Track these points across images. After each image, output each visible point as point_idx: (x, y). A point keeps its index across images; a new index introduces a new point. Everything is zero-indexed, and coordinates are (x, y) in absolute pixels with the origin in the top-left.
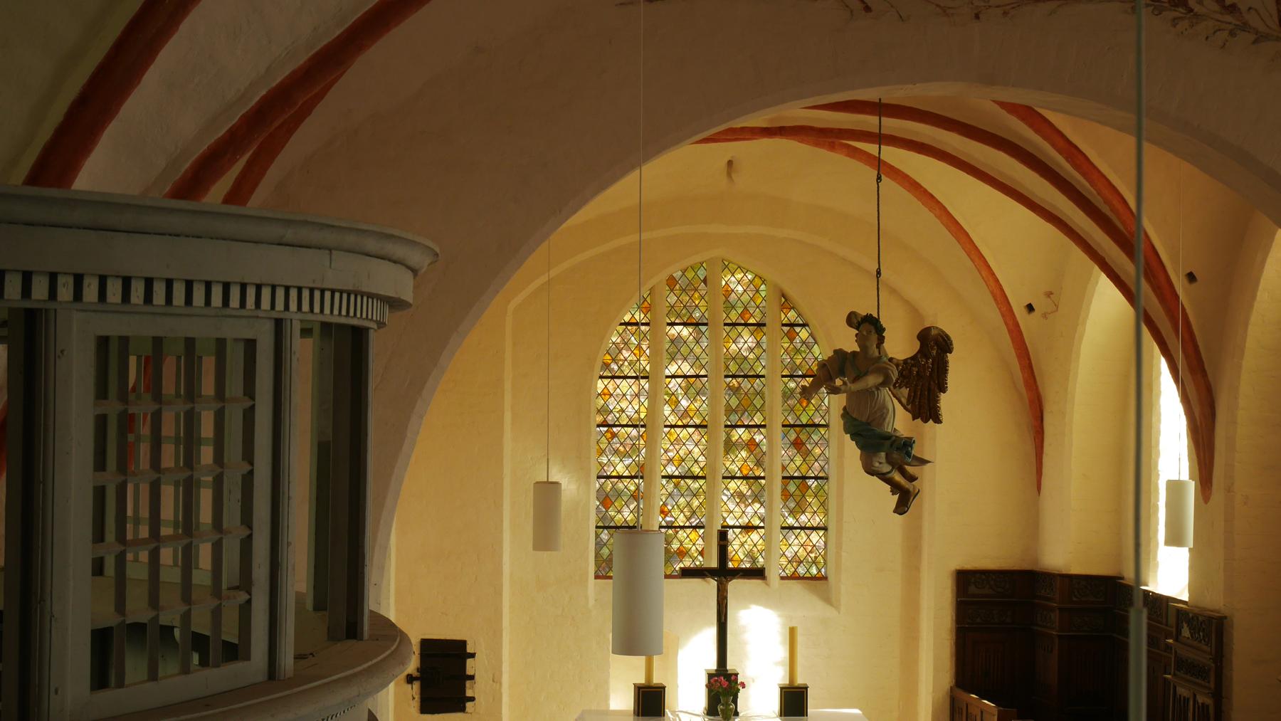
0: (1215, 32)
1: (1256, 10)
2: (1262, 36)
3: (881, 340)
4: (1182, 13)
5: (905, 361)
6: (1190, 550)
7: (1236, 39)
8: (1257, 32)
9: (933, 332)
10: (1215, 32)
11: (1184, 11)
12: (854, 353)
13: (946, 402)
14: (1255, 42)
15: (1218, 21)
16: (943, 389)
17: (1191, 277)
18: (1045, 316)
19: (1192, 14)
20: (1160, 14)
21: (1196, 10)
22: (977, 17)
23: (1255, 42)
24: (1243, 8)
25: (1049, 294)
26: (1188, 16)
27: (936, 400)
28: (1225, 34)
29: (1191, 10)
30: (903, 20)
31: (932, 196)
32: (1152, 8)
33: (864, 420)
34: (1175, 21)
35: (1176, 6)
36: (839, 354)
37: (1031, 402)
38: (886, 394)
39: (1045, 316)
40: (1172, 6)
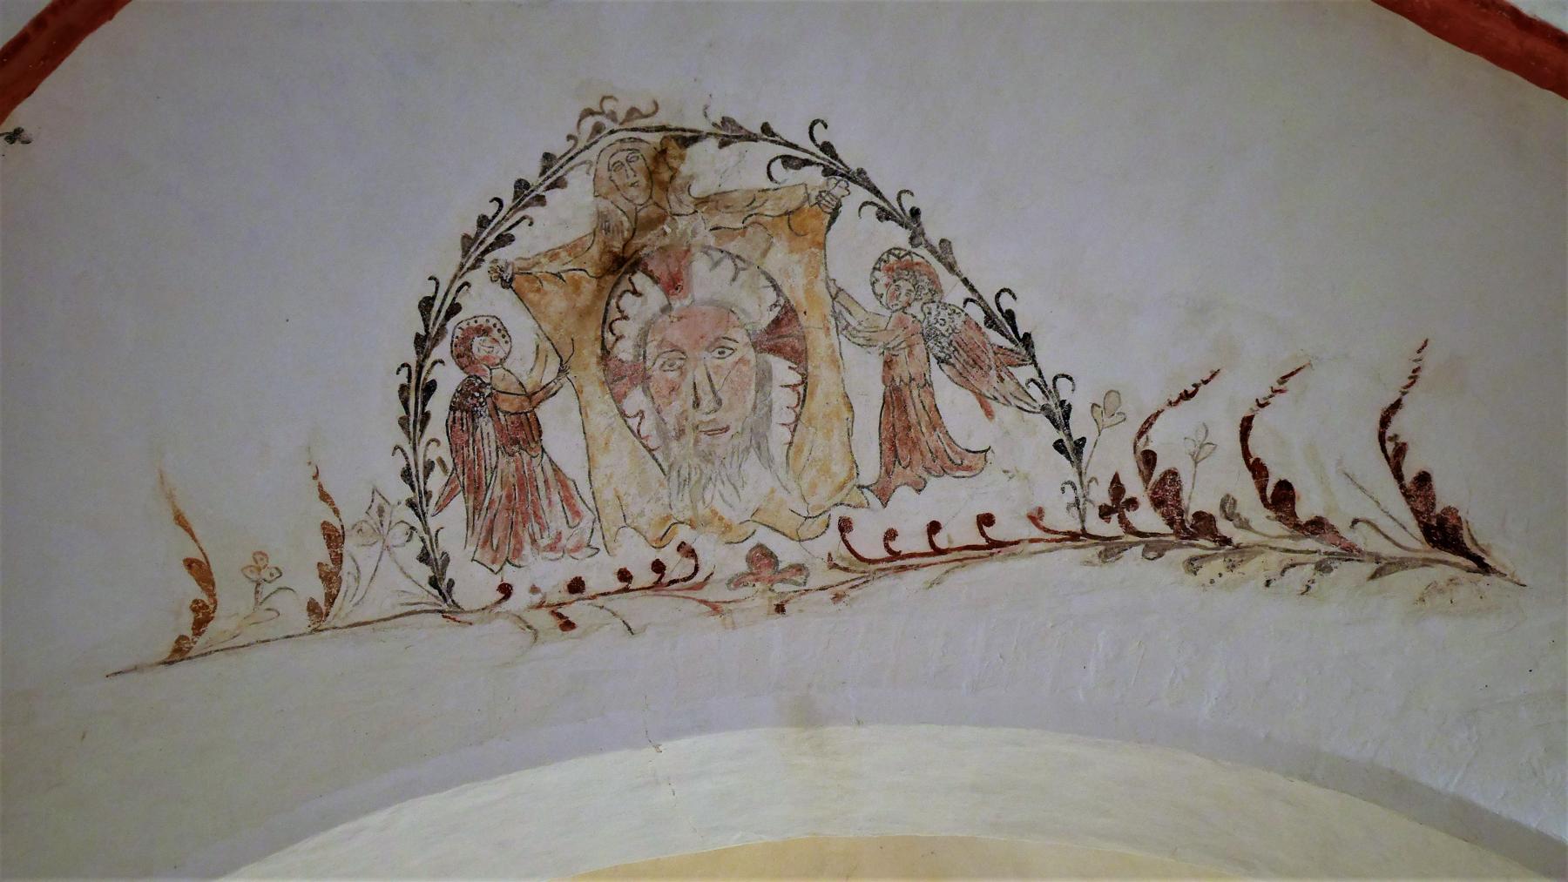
0: (1284, 571)
1: (1368, 522)
2: (1390, 564)
4: (1200, 547)
7: (1332, 574)
8: (1378, 559)
10: (1284, 571)
11: (1210, 545)
14: (1373, 577)
15: (1288, 551)
19: (1228, 547)
20: (1160, 556)
21: (1235, 541)
22: (780, 609)
23: (1373, 577)
24: (1341, 525)
26: (1221, 551)
28: (1308, 570)
29: (1226, 541)
30: (633, 634)
32: (1142, 546)
34: (1193, 565)
35: (1193, 536)
40: (1183, 538)
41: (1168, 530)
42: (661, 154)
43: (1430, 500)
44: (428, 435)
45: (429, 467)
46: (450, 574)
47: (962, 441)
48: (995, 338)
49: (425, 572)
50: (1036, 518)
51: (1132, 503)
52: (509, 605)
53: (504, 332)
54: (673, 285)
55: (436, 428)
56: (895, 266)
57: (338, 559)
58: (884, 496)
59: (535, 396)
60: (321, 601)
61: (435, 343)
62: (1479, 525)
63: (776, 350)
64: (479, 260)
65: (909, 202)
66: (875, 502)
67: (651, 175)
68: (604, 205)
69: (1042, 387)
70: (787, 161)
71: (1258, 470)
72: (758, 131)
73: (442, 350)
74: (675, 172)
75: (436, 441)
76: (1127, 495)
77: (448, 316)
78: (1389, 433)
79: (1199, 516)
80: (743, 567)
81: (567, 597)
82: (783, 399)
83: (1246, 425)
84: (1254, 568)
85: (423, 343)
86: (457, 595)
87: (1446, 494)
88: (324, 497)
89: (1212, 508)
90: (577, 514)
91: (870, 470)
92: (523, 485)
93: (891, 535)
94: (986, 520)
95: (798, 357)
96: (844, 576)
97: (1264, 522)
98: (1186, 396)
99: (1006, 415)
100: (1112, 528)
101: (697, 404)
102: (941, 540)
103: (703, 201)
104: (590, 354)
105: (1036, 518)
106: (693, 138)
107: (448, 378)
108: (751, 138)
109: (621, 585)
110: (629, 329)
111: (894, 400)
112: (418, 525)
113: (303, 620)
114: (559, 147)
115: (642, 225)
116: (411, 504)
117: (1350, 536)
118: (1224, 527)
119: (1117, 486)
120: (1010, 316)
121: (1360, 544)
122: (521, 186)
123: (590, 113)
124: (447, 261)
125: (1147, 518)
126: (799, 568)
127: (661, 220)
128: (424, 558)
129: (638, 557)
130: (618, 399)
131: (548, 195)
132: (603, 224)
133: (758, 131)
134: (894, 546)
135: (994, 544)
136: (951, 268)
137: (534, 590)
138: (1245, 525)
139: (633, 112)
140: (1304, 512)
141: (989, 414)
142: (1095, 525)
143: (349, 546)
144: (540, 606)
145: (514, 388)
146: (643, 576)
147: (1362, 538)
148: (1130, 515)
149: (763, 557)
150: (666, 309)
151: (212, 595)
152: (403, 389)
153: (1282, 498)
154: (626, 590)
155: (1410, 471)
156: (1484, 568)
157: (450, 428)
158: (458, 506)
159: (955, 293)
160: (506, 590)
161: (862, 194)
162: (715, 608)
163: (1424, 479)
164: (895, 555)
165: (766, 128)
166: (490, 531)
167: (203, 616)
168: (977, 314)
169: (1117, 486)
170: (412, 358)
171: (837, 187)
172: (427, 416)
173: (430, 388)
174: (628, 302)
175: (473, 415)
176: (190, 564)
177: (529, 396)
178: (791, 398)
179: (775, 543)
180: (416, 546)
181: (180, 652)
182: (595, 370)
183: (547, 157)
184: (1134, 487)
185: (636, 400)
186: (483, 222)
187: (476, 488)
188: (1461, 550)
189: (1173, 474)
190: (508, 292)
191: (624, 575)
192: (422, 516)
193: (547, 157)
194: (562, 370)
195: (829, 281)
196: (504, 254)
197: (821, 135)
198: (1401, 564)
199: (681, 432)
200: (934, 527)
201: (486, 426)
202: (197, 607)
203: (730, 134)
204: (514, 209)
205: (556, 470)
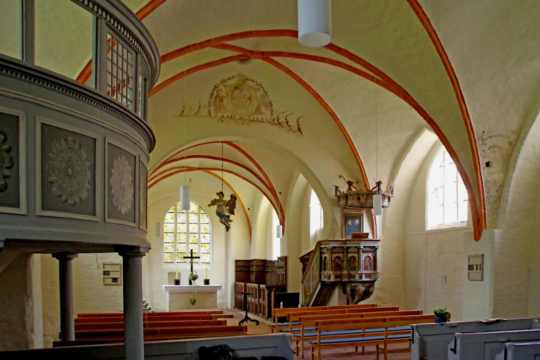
3: (223, 197)
5: (228, 201)
6: (281, 238)
8: (294, 131)
9: (233, 195)
12: (218, 199)
13: (235, 210)
14: (294, 132)
16: (235, 208)
17: (280, 193)
18: (252, 211)
23: (294, 132)
25: (252, 206)
27: (234, 210)
29: (282, 126)
31: (230, 186)
33: (220, 212)
34: (279, 128)
35: (280, 124)
36: (215, 199)
37: (249, 228)
38: (224, 207)
39: (252, 211)
41: (277, 123)
42: (245, 80)
43: (299, 126)
44: (212, 99)
45: (211, 102)
46: (211, 113)
47: (263, 112)
48: (269, 104)
49: (208, 112)
50: (267, 120)
51: (275, 120)
52: (216, 117)
53: (222, 91)
54: (241, 91)
55: (213, 99)
56: (263, 96)
57: (200, 109)
58: (254, 114)
59: (223, 97)
60: (197, 113)
61: (215, 90)
62: (302, 130)
63: (248, 100)
64: (222, 83)
65: (267, 91)
66: (253, 115)
67: (243, 81)
68: (237, 82)
69: (271, 109)
70: (257, 85)
71: (286, 119)
72: (255, 81)
73: (215, 91)
74: (245, 82)
75: (213, 100)
76: (275, 119)
77: (217, 87)
78: (298, 120)
79: (280, 122)
80: (239, 118)
81: (222, 117)
82: (248, 104)
83: (287, 116)
84: (284, 129)
85: (213, 89)
86: (211, 115)
87: (301, 126)
88: (200, 103)
89: (281, 122)
90: (225, 109)
91: (253, 112)
92: (220, 106)
93: (254, 118)
94: (262, 119)
95: (251, 101)
96: (249, 121)
97: (285, 125)
98: (283, 113)
99: (267, 111)
100: (273, 122)
101: (239, 102)
102: (258, 119)
103: (247, 85)
104: (230, 94)
105: (267, 120)
106: (249, 80)
107: (215, 94)
108: (255, 82)
109: (227, 117)
110: (235, 94)
111: (258, 107)
112: (209, 107)
113: (194, 114)
114: (234, 76)
115: (240, 85)
116: (209, 106)
117: (292, 128)
118: (282, 124)
119: (274, 118)
120: (271, 103)
121: (293, 129)
122: (229, 78)
123: (239, 74)
124: (218, 82)
125: (276, 122)
126: (244, 119)
127: (242, 85)
128: (209, 111)
129: (229, 115)
130: (232, 100)
131: (232, 80)
132: (236, 84)
133: (255, 81)
134: (254, 119)
135: (262, 121)
136: (268, 98)
137: (219, 116)
138: (284, 124)
139: (243, 75)
140: (289, 125)
141: (266, 110)
142: (271, 121)
143: (201, 108)
144: (219, 118)
145: (222, 96)
146: (230, 117)
147: (293, 128)
148: (275, 121)
149: (241, 117)
150: (240, 93)
151: (184, 109)
152: (211, 94)
153: (287, 122)
154: (228, 118)
155: (298, 124)
156: (302, 134)
157: (214, 99)
158: (213, 107)
159: (267, 99)
160: (216, 116)
161: (263, 89)
162: (237, 122)
163: (299, 124)
164: (253, 120)
165: (256, 82)
166: (216, 110)
167: (183, 111)
168: (268, 102)
169: (274, 118)
170: (212, 91)
171: (261, 88)
172: (212, 97)
173: (213, 94)
174: (236, 91)
175: (217, 98)
176: (183, 106)
177: (223, 97)
178: (248, 104)
179: (243, 116)
180: (208, 109)
181: (181, 116)
182: (230, 96)
183: (233, 76)
184: (276, 119)
185: (234, 100)
186: (224, 80)
187: (215, 105)
188: (300, 132)
189: (279, 118)
190: (224, 87)
191: (228, 116)
192: (209, 107)
193: (233, 76)
194: (227, 96)
195: (256, 95)
196: (225, 83)
197: (261, 84)
198: (296, 132)
199: (237, 105)
200: (258, 118)
201: (218, 99)
202: (183, 110)
203: (253, 81)
204: (228, 80)
205: (224, 105)
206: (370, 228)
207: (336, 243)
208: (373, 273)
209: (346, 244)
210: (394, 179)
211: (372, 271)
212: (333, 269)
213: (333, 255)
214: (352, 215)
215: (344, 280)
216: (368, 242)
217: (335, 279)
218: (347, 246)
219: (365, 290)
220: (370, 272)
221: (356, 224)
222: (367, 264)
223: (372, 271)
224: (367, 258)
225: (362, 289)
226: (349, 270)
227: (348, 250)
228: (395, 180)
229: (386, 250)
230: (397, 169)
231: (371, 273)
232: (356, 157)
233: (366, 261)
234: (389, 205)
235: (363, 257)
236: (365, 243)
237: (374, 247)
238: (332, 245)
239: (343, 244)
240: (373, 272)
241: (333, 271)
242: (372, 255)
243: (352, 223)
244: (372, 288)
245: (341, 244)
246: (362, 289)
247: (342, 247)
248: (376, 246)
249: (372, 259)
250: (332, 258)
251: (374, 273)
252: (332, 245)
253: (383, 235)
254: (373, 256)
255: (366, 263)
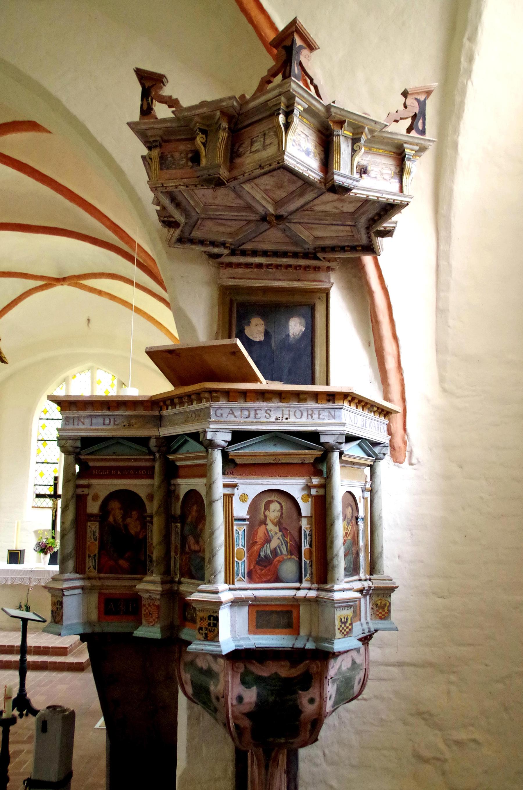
206: (371, 358)
207: (104, 417)
208: (306, 600)
209: (159, 421)
210: (458, 99)
211: (305, 584)
212: (90, 563)
213: (94, 482)
214: (260, 298)
215: (141, 632)
216: (265, 405)
217: (100, 618)
218: (166, 431)
219: (261, 703)
220: (290, 593)
221: (288, 335)
222: (274, 543)
223: (305, 584)
224: (275, 507)
225: (240, 699)
226: (182, 575)
227: (171, 457)
228: (462, 104)
229: (461, 467)
230: (465, 40)
231: (294, 599)
232: (251, 20)
233: (264, 522)
234: (401, 190)
235: (243, 498)
236: (242, 409)
237: (314, 436)
238: (81, 426)
239: (146, 421)
240: (313, 594)
241: (94, 573)
242: (308, 487)
243: (267, 334)
244: (313, 692)
245: (130, 425)
246: (240, 699)
247: (144, 441)
248: (325, 433)
249: (306, 509)
250: (236, 500)
251: (316, 600)
252: (81, 426)
253: (444, 390)
254: (313, 492)
255: (261, 532)
